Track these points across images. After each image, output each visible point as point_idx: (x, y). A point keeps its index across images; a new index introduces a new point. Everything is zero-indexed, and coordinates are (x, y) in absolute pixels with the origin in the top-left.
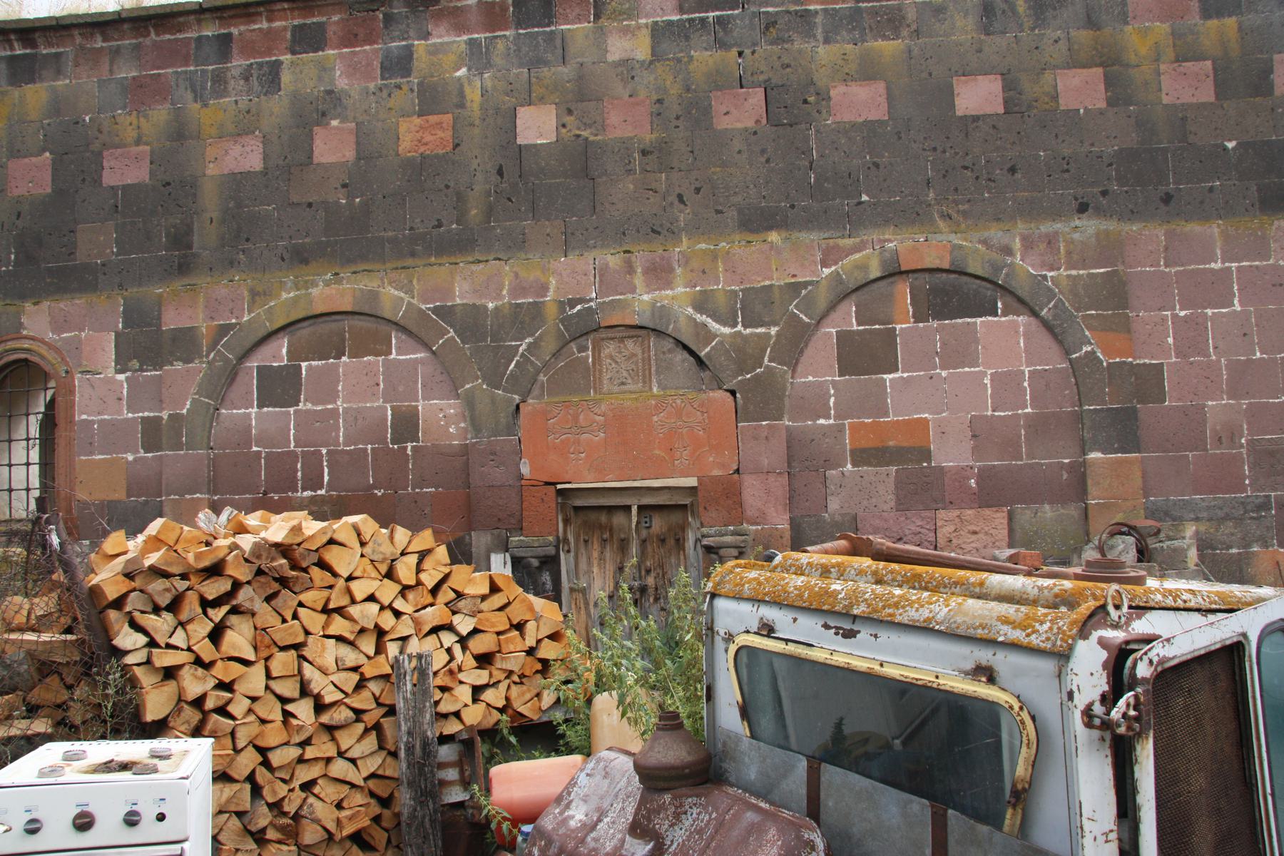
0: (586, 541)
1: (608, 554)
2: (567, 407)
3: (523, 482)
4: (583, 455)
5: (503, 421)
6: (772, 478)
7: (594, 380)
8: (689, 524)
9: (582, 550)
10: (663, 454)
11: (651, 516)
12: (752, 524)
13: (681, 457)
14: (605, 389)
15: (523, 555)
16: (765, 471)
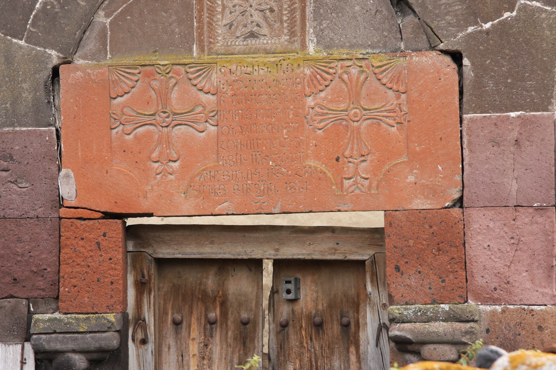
0: (177, 324)
1: (216, 348)
2: (148, 75)
3: (63, 212)
4: (175, 165)
6: (524, 217)
7: (200, 28)
8: (368, 296)
9: (170, 340)
10: (323, 167)
11: (297, 281)
12: (485, 301)
13: (356, 173)
14: (219, 46)
15: (59, 347)
16: (514, 202)
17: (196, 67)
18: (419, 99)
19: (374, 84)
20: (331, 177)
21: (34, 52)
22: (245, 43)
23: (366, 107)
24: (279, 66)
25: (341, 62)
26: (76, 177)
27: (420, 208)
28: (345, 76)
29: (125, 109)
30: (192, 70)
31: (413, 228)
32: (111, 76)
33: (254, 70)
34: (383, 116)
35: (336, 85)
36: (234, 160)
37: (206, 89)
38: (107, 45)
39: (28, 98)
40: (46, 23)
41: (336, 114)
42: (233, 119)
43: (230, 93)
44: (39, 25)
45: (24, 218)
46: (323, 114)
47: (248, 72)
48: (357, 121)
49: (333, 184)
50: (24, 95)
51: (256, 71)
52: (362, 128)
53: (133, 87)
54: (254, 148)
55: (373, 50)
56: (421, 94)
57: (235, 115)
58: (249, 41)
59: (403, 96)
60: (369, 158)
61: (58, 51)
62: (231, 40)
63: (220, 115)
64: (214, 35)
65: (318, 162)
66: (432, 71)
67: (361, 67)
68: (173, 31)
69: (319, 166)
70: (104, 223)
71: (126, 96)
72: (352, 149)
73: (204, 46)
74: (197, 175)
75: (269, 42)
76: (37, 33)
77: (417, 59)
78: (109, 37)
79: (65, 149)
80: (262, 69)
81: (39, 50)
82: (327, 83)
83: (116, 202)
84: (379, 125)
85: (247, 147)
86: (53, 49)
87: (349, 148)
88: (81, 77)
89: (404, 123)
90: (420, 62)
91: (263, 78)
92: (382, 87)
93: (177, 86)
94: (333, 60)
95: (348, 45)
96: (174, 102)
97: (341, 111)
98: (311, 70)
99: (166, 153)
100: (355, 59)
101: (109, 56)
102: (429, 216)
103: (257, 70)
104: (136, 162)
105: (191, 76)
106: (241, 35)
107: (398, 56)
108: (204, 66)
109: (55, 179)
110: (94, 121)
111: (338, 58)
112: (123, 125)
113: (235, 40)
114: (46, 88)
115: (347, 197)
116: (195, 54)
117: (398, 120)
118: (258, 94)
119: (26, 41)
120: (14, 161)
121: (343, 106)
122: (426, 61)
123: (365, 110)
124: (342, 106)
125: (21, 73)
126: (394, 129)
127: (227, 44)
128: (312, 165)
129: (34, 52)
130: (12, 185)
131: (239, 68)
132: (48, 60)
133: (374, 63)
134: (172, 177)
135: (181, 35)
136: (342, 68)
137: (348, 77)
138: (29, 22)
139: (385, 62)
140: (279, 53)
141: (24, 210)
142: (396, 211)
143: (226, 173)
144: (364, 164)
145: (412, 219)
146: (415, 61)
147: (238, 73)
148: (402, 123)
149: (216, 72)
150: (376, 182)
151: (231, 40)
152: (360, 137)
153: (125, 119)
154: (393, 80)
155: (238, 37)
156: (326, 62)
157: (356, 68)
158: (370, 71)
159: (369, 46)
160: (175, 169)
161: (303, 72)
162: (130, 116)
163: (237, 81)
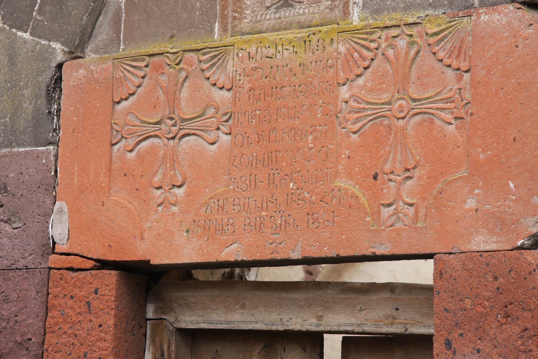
2: (158, 69)
3: (53, 260)
4: (180, 192)
5: (28, 106)
10: (356, 191)
13: (398, 197)
17: (210, 52)
18: (487, 79)
19: (427, 60)
20: (366, 203)
21: (38, 47)
22: (277, 15)
23: (416, 96)
24: (308, 43)
25: (386, 31)
26: (70, 211)
27: (482, 248)
28: (390, 52)
29: (128, 117)
30: (205, 57)
31: (471, 280)
32: (116, 73)
33: (278, 51)
34: (437, 109)
35: (379, 66)
36: (248, 182)
37: (220, 83)
38: (121, 32)
39: (28, 108)
40: (53, 8)
41: (376, 109)
42: (248, 123)
43: (247, 86)
44: (46, 11)
45: (13, 269)
46: (360, 110)
47: (269, 55)
48: (403, 118)
49: (367, 214)
50: (25, 105)
51: (279, 52)
52: (409, 128)
53: (139, 86)
54: (272, 164)
55: (435, 11)
56: (489, 71)
57: (252, 118)
58: (283, 13)
59: (466, 76)
60: (417, 173)
61: (63, 44)
62: (261, 13)
63: (234, 118)
64: (241, 8)
65: (351, 182)
66: (506, 34)
67: (411, 36)
68: (193, 7)
69: (351, 188)
70: (97, 275)
71: (131, 99)
72: (394, 160)
73: (227, 23)
74: (203, 205)
75: (306, 11)
76: (43, 22)
77: (487, 17)
78: (123, 22)
79: (61, 174)
80: (287, 49)
81: (44, 44)
82: (366, 64)
83: (110, 246)
84: (432, 122)
85: (264, 162)
86: (57, 41)
87: (390, 159)
88: (84, 76)
89: (465, 117)
90: (490, 21)
91: (287, 62)
92: (438, 65)
93: (188, 80)
94: (375, 29)
95: (402, 6)
96: (183, 103)
97: (383, 104)
98: (347, 46)
99: (169, 175)
100: (405, 25)
101: (122, 47)
102: (493, 261)
103: (281, 52)
104: (137, 189)
105: (204, 66)
106: (272, 5)
107: (460, 15)
108: (219, 50)
109: (48, 215)
110: (93, 136)
111: (381, 25)
112: (126, 138)
113: (266, 12)
114: (49, 94)
115: (384, 234)
116: (216, 36)
117: (457, 113)
118: (279, 87)
119: (31, 34)
120: (8, 193)
121: (385, 97)
122: (498, 20)
123: (414, 100)
124: (384, 97)
125: (23, 76)
126: (452, 128)
127: (256, 19)
128: (341, 186)
129: (38, 47)
130: (5, 225)
131: (259, 49)
132: (51, 57)
133: (429, 28)
134: (175, 209)
135: (202, 10)
136: (386, 40)
137: (394, 53)
138: (36, 8)
139: (444, 27)
140: (316, 26)
141: (14, 258)
142: (450, 253)
143: (237, 201)
144: (410, 183)
145: (471, 266)
146: (483, 22)
147: (258, 57)
148: (463, 118)
149: (233, 59)
150: (424, 210)
151: (261, 13)
152: (405, 141)
153: (127, 130)
154: (452, 52)
155: (268, 8)
156: (367, 33)
157: (405, 38)
158: (423, 42)
159: (430, 5)
160: (179, 198)
161: (336, 50)
162: (133, 126)
163: (256, 68)
